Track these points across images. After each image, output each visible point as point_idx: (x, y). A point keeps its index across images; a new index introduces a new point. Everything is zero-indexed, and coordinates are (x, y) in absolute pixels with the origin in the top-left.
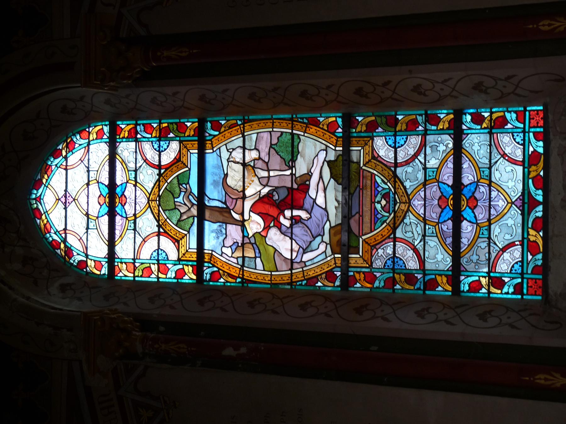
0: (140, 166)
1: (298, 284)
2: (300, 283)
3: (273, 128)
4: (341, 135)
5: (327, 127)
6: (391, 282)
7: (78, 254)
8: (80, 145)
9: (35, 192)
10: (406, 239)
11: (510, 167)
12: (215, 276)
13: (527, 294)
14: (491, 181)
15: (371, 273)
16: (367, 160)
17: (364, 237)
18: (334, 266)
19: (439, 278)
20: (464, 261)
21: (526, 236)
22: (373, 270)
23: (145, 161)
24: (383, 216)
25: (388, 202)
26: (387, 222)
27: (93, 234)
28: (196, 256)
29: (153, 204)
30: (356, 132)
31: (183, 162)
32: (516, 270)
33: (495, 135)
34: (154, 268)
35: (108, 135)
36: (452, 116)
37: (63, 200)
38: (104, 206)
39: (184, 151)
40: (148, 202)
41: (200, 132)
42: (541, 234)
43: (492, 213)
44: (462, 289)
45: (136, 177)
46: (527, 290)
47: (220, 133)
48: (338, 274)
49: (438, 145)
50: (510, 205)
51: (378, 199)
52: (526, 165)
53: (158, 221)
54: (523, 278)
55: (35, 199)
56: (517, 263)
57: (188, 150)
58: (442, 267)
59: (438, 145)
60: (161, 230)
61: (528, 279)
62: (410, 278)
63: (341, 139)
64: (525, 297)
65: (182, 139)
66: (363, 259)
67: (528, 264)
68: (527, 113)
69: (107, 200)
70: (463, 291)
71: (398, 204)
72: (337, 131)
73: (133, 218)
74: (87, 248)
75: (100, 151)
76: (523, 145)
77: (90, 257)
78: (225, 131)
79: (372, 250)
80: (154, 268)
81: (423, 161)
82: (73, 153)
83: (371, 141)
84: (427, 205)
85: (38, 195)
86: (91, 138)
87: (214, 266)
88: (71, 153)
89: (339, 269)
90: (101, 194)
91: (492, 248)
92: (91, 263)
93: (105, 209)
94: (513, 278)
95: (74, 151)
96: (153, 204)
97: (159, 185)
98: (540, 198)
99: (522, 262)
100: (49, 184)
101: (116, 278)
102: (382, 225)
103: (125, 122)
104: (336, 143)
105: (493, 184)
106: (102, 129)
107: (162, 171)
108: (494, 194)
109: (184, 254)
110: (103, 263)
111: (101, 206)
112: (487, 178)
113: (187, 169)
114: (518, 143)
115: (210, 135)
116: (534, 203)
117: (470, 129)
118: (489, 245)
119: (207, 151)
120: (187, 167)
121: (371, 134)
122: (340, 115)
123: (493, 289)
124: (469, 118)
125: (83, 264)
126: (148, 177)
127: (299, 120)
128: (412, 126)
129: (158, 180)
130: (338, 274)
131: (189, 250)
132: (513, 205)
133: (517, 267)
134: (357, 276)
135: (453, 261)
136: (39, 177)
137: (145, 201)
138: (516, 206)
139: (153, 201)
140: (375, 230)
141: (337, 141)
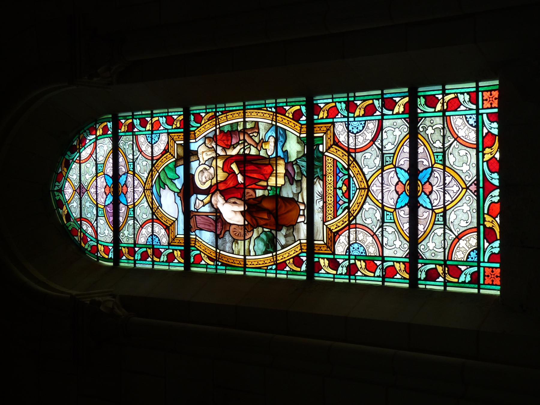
0: (137, 158)
1: (269, 268)
2: (271, 267)
6: (352, 270)
7: (91, 240)
8: (90, 140)
9: (57, 184)
10: (366, 225)
15: (335, 259)
16: (329, 145)
17: (326, 224)
18: (300, 251)
19: (397, 266)
20: (421, 247)
21: (482, 222)
22: (336, 257)
24: (345, 202)
30: (318, 119)
31: (170, 153)
32: (472, 258)
33: (448, 118)
34: (150, 252)
36: (407, 99)
37: (78, 191)
38: (109, 196)
39: (171, 143)
40: (144, 192)
41: (186, 124)
42: (498, 219)
43: (447, 199)
44: (419, 277)
45: (134, 168)
46: (484, 279)
47: (201, 125)
48: (304, 259)
50: (464, 190)
51: (340, 184)
54: (479, 267)
55: (57, 191)
56: (473, 251)
58: (400, 254)
60: (155, 217)
61: (484, 267)
63: (305, 126)
65: (170, 131)
68: (480, 93)
69: (112, 190)
70: (420, 279)
71: (358, 190)
72: (301, 119)
75: (105, 146)
76: (477, 126)
77: (100, 242)
78: (205, 123)
79: (335, 236)
80: (150, 252)
81: (380, 147)
82: (85, 148)
84: (384, 191)
85: (60, 186)
86: (98, 134)
88: (83, 148)
89: (305, 254)
91: (447, 235)
92: (101, 248)
94: (471, 267)
95: (86, 146)
97: (152, 176)
98: (496, 182)
100: (67, 177)
102: (343, 212)
104: (301, 130)
105: (447, 169)
107: (154, 162)
108: (448, 179)
110: (111, 248)
112: (441, 162)
114: (472, 125)
116: (489, 188)
117: (425, 112)
118: (444, 231)
119: (191, 141)
121: (331, 120)
124: (423, 100)
125: (95, 249)
127: (268, 109)
128: (370, 111)
129: (151, 170)
130: (304, 259)
131: (178, 236)
132: (468, 190)
133: (473, 255)
134: (322, 261)
135: (410, 248)
136: (60, 170)
137: (141, 189)
138: (471, 191)
140: (337, 217)
141: (301, 128)
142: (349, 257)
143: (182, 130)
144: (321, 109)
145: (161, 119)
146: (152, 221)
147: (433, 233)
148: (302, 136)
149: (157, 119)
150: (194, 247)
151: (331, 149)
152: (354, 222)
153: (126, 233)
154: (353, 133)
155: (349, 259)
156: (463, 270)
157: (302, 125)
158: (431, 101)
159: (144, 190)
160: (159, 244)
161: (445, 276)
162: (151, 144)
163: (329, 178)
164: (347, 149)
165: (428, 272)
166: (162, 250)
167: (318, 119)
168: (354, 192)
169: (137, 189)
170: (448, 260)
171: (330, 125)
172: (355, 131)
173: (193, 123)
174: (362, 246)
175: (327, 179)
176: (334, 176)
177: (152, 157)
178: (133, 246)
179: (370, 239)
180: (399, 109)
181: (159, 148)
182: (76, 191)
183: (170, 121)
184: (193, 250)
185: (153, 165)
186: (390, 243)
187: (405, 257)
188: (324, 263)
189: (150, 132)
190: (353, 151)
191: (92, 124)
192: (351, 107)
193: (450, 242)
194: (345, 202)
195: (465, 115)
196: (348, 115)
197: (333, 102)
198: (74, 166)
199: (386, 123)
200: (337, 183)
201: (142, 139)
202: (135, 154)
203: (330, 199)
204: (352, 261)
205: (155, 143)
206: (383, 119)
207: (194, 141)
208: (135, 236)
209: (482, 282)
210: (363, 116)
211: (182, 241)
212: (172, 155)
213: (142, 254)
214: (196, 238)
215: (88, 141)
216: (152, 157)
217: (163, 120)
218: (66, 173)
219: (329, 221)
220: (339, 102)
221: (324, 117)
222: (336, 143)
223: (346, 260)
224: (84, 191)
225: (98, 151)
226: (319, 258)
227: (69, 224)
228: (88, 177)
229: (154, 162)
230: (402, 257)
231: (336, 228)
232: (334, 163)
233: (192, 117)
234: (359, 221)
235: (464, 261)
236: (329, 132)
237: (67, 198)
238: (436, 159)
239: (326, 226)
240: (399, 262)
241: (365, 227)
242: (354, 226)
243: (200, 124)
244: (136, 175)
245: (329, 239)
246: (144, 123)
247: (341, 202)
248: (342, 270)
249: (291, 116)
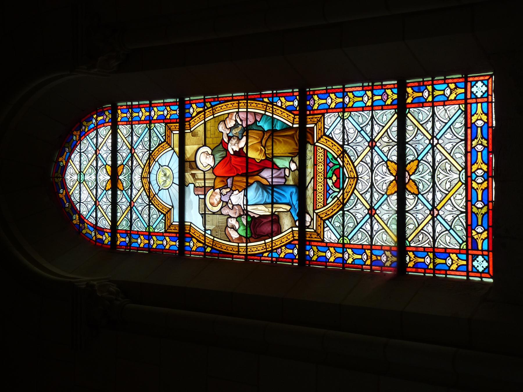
3: (239, 108)
17: (316, 211)
24: (334, 192)
25: (338, 178)
26: (338, 196)
31: (167, 143)
51: (330, 174)
57: (172, 132)
66: (317, 233)
71: (347, 179)
96: (145, 181)
97: (149, 163)
104: (294, 120)
109: (169, 227)
141: (294, 118)
151: (322, 140)
163: (320, 167)
171: (320, 116)
175: (318, 167)
176: (324, 165)
185: (150, 154)
194: (334, 192)
200: (327, 173)
203: (320, 188)
211: (177, 228)
214: (190, 225)
219: (319, 209)
231: (326, 216)
236: (319, 123)
239: (317, 214)
247: (331, 192)
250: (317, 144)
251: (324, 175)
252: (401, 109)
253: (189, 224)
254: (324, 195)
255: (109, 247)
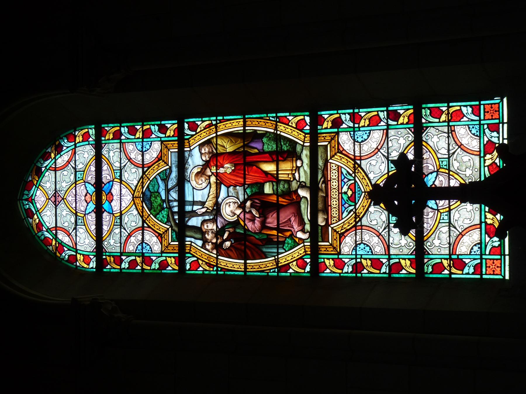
0: (125, 166)
1: (271, 271)
4: (308, 131)
5: (296, 125)
6: (358, 267)
7: (69, 250)
8: (68, 147)
9: (26, 192)
11: (466, 158)
12: (196, 265)
13: (486, 274)
14: (449, 170)
17: (332, 226)
19: (403, 262)
21: (483, 220)
23: (129, 160)
27: (81, 230)
28: (177, 249)
29: (137, 201)
32: (475, 252)
33: (453, 127)
34: (139, 260)
35: (94, 138)
37: (53, 199)
40: (133, 200)
41: (180, 132)
44: (426, 271)
45: (121, 176)
47: (196, 133)
49: (398, 138)
51: (345, 189)
52: (482, 155)
53: (142, 217)
54: (481, 259)
56: (475, 245)
57: (169, 150)
58: (406, 251)
59: (398, 138)
60: (145, 225)
61: (486, 259)
62: (376, 264)
64: (484, 277)
67: (486, 246)
70: (427, 273)
73: (119, 214)
74: (76, 244)
75: (86, 153)
77: (79, 251)
78: (201, 131)
81: (386, 155)
82: (61, 156)
83: (336, 136)
87: (194, 256)
88: (59, 155)
90: (88, 192)
93: (92, 206)
95: (62, 154)
97: (143, 182)
99: (480, 243)
101: (105, 270)
102: (348, 215)
103: (110, 125)
106: (88, 132)
107: (145, 169)
110: (92, 257)
111: (88, 203)
112: (445, 167)
113: (168, 167)
115: (188, 135)
119: (186, 149)
120: (168, 165)
121: (336, 130)
122: (307, 113)
123: (454, 270)
125: (73, 259)
126: (132, 176)
127: (271, 118)
128: (374, 121)
129: (142, 177)
133: (476, 248)
134: (327, 262)
137: (130, 197)
139: (137, 197)
140: (342, 219)
141: (305, 137)
142: (356, 256)
143: (176, 138)
144: (325, 119)
145: (152, 127)
146: (143, 228)
147: (439, 231)
148: (305, 144)
149: (148, 127)
150: (189, 253)
151: (336, 157)
152: (359, 224)
153: (437, 242)
154: (357, 142)
155: (356, 258)
156: (467, 262)
157: (306, 134)
158: (436, 113)
159: (133, 197)
160: (150, 252)
161: (450, 269)
162: (142, 151)
164: (353, 157)
165: (433, 266)
166: (154, 258)
167: (322, 129)
168: (359, 196)
169: (101, 198)
170: (453, 254)
171: (334, 134)
172: (360, 140)
173: (187, 132)
174: (368, 246)
175: (332, 184)
177: (143, 164)
178: (119, 254)
179: (376, 239)
180: (403, 120)
181: (151, 155)
182: (49, 199)
183: (163, 129)
184: (189, 257)
186: (396, 242)
187: (411, 254)
188: (329, 263)
189: (141, 140)
190: (358, 158)
191: (72, 131)
192: (355, 118)
193: (454, 238)
194: (350, 206)
195: (468, 125)
196: (354, 125)
197: (338, 113)
198: (47, 174)
199: (391, 132)
201: (130, 147)
202: (122, 162)
204: (359, 260)
205: (146, 151)
206: (387, 130)
207: (189, 149)
208: (452, 247)
209: (484, 272)
210: (368, 126)
212: (165, 163)
213: (130, 263)
214: (191, 245)
215: (65, 148)
216: (143, 164)
217: (155, 129)
218: (37, 181)
219: (334, 223)
220: (343, 114)
221: (329, 127)
222: (340, 151)
223: (352, 259)
224: (60, 199)
225: (77, 158)
226: (324, 259)
227: (40, 234)
228: (64, 184)
229: (145, 169)
230: (407, 255)
232: (338, 169)
233: (186, 126)
234: (364, 222)
235: (467, 255)
236: (333, 141)
237: (39, 206)
238: (441, 164)
240: (405, 259)
241: (370, 228)
242: (360, 227)
243: (196, 131)
244: (123, 183)
245: (335, 240)
246: (132, 131)
248: (348, 269)
249: (294, 125)
250: (330, 161)
251: (338, 191)
252: (418, 129)
253: (190, 243)
254: (339, 210)
255: (95, 270)
